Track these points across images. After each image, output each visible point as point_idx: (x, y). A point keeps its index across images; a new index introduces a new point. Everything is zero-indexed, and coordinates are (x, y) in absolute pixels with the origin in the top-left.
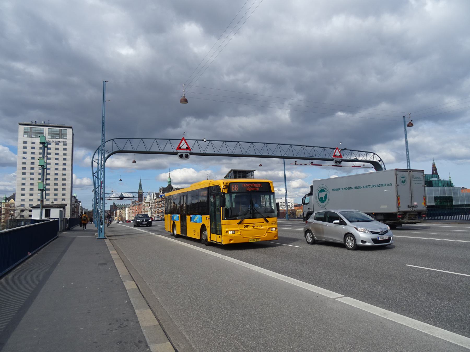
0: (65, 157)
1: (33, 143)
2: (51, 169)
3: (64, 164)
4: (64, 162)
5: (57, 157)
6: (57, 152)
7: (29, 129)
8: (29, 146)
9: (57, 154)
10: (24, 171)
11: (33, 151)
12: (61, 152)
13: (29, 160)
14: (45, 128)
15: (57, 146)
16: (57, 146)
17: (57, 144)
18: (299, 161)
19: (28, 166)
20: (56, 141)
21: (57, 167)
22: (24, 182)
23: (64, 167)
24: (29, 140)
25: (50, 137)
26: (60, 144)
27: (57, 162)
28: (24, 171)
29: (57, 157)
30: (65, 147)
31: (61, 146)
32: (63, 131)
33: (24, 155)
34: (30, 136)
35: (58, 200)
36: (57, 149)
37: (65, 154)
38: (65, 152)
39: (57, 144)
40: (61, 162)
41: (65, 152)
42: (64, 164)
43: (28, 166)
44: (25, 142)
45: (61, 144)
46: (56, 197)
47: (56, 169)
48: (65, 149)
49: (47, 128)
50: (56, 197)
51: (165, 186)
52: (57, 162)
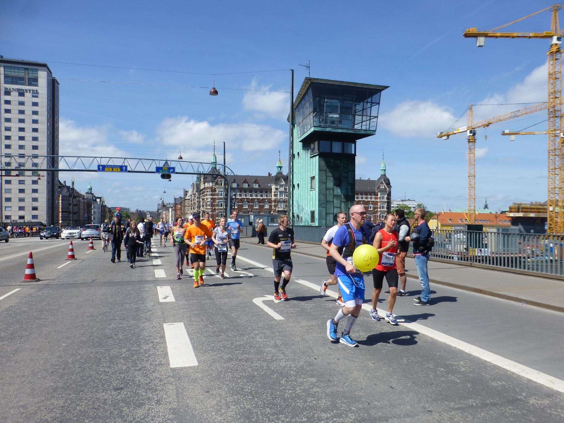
0: (35, 117)
2: (12, 138)
3: (35, 130)
4: (35, 126)
5: (22, 117)
6: (21, 108)
9: (22, 112)
12: (29, 109)
16: (21, 99)
17: (21, 94)
20: (18, 90)
23: (35, 134)
26: (26, 94)
27: (22, 125)
29: (22, 117)
30: (35, 100)
35: (26, 191)
37: (35, 113)
38: (35, 109)
39: (21, 94)
40: (29, 126)
42: (35, 130)
45: (28, 95)
46: (35, 187)
47: (22, 138)
48: (35, 104)
50: (35, 187)
51: (207, 169)
52: (22, 125)
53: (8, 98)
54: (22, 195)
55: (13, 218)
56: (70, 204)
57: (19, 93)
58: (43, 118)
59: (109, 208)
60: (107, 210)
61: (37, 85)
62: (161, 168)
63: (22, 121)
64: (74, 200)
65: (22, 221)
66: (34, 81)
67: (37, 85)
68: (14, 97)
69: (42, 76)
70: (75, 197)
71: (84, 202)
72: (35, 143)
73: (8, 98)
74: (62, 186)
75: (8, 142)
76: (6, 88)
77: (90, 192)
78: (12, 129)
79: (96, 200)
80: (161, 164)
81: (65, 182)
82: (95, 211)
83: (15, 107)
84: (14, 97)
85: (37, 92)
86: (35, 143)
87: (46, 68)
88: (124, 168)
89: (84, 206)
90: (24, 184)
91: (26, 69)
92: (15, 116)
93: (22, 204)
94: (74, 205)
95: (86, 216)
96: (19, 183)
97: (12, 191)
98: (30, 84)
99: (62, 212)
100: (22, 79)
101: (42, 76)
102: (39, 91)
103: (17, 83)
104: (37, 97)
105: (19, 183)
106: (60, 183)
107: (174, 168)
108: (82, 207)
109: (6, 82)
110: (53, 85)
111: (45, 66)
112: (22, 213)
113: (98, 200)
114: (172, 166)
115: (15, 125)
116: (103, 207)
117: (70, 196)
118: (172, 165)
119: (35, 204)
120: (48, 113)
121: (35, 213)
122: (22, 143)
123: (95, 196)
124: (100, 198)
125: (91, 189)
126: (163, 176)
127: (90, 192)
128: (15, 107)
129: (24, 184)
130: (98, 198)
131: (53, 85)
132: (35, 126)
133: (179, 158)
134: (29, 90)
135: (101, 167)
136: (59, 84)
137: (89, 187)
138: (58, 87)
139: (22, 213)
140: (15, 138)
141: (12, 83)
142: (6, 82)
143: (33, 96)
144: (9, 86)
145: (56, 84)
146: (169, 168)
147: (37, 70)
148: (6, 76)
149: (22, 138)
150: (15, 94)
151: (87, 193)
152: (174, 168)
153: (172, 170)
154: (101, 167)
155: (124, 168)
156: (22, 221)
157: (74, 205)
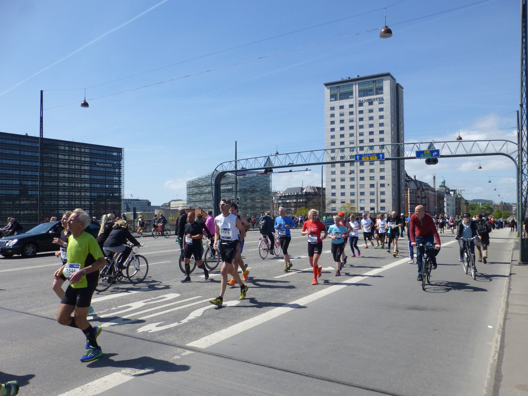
0: (381, 121)
1: (342, 107)
8: (337, 112)
11: (342, 118)
12: (376, 114)
16: (371, 107)
17: (371, 103)
20: (369, 100)
24: (337, 104)
26: (374, 102)
30: (381, 106)
31: (376, 105)
36: (371, 111)
38: (381, 113)
39: (371, 103)
41: (381, 113)
44: (332, 109)
45: (376, 103)
53: (361, 108)
55: (366, 209)
56: (418, 197)
57: (369, 103)
58: (387, 121)
59: (466, 201)
60: (463, 202)
61: (382, 93)
62: (422, 152)
64: (423, 193)
66: (380, 90)
67: (382, 93)
68: (366, 107)
69: (387, 85)
70: (423, 190)
71: (435, 195)
73: (361, 108)
74: (409, 179)
76: (360, 101)
77: (443, 185)
79: (449, 193)
80: (424, 148)
81: (415, 176)
82: (447, 204)
83: (366, 115)
84: (366, 107)
85: (382, 99)
87: (389, 77)
88: (381, 155)
89: (435, 199)
90: (374, 179)
91: (374, 82)
92: (366, 122)
94: (423, 198)
95: (436, 207)
96: (370, 179)
97: (365, 186)
98: (377, 94)
99: (411, 204)
100: (371, 90)
101: (387, 85)
102: (384, 98)
103: (367, 95)
104: (383, 103)
105: (370, 179)
106: (409, 177)
107: (438, 151)
108: (432, 199)
109: (360, 96)
110: (397, 90)
111: (388, 75)
113: (452, 193)
114: (437, 148)
116: (459, 200)
117: (418, 189)
118: (437, 147)
119: (383, 197)
120: (392, 116)
121: (383, 205)
123: (449, 189)
124: (454, 191)
125: (444, 182)
126: (429, 162)
127: (443, 185)
128: (366, 115)
129: (374, 179)
130: (452, 191)
131: (397, 90)
132: (381, 129)
133: (458, 139)
134: (377, 99)
135: (358, 157)
136: (402, 88)
137: (442, 180)
138: (402, 91)
141: (364, 96)
142: (360, 96)
143: (380, 103)
144: (362, 99)
145: (400, 89)
146: (432, 152)
147: (382, 80)
148: (360, 91)
150: (366, 104)
151: (440, 186)
152: (438, 151)
153: (436, 153)
154: (358, 157)
155: (381, 155)
156: (372, 212)
157: (423, 198)
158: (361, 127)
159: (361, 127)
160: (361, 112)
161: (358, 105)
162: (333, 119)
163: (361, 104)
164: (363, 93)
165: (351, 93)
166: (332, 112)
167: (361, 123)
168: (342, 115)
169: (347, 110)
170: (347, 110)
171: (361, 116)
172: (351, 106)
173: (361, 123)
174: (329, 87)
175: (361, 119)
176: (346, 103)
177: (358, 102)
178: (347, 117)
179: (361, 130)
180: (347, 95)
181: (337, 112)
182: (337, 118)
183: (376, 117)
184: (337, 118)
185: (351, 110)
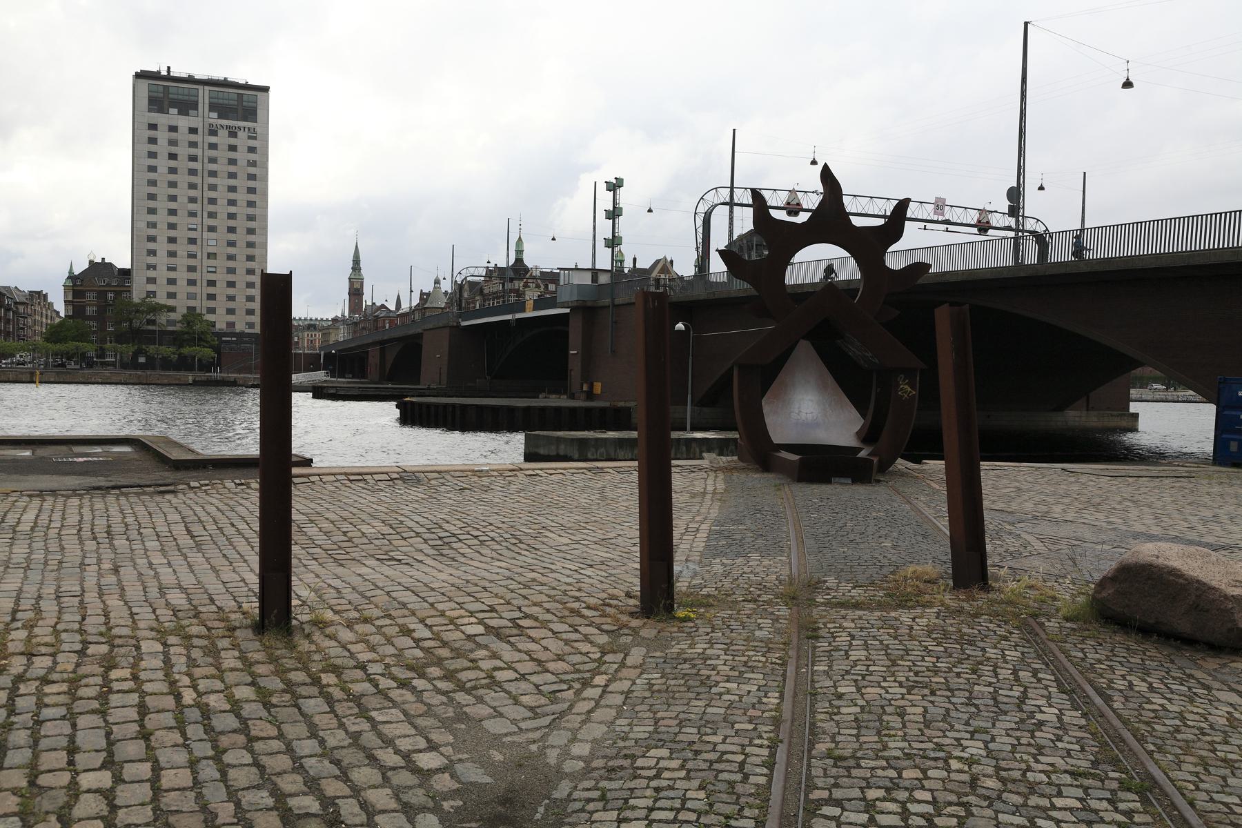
1: (173, 129)
2: (219, 201)
5: (232, 169)
6: (232, 155)
7: (161, 89)
8: (163, 136)
10: (152, 204)
11: (173, 150)
13: (162, 175)
14: (200, 87)
15: (233, 141)
16: (233, 141)
17: (233, 134)
18: (929, 225)
19: (162, 190)
21: (232, 196)
22: (152, 232)
24: (162, 119)
25: (215, 115)
26: (240, 134)
28: (152, 204)
29: (232, 169)
30: (252, 143)
32: (245, 98)
33: (152, 162)
34: (162, 110)
39: (233, 134)
43: (162, 190)
44: (153, 127)
49: (207, 88)
52: (232, 182)
53: (213, 139)
54: (231, 291)
55: (218, 326)
63: (232, 175)
65: (230, 330)
68: (222, 139)
72: (251, 211)
73: (213, 139)
75: (211, 208)
78: (219, 188)
84: (222, 139)
86: (251, 211)
93: (231, 305)
98: (245, 119)
104: (255, 138)
112: (231, 318)
115: (222, 182)
122: (232, 210)
128: (223, 154)
139: (231, 318)
140: (222, 202)
143: (250, 138)
149: (232, 203)
150: (223, 133)
158: (213, 174)
159: (213, 174)
160: (213, 146)
161: (206, 131)
162: (153, 148)
163: (213, 132)
164: (223, 110)
165: (194, 106)
166: (152, 133)
167: (213, 167)
168: (173, 143)
169: (183, 136)
170: (183, 136)
171: (213, 153)
172: (193, 131)
173: (213, 167)
174: (144, 84)
175: (213, 160)
176: (184, 123)
177: (207, 126)
178: (183, 151)
179: (212, 181)
180: (187, 107)
181: (163, 136)
182: (162, 148)
183: (242, 162)
184: (162, 148)
185: (193, 137)
